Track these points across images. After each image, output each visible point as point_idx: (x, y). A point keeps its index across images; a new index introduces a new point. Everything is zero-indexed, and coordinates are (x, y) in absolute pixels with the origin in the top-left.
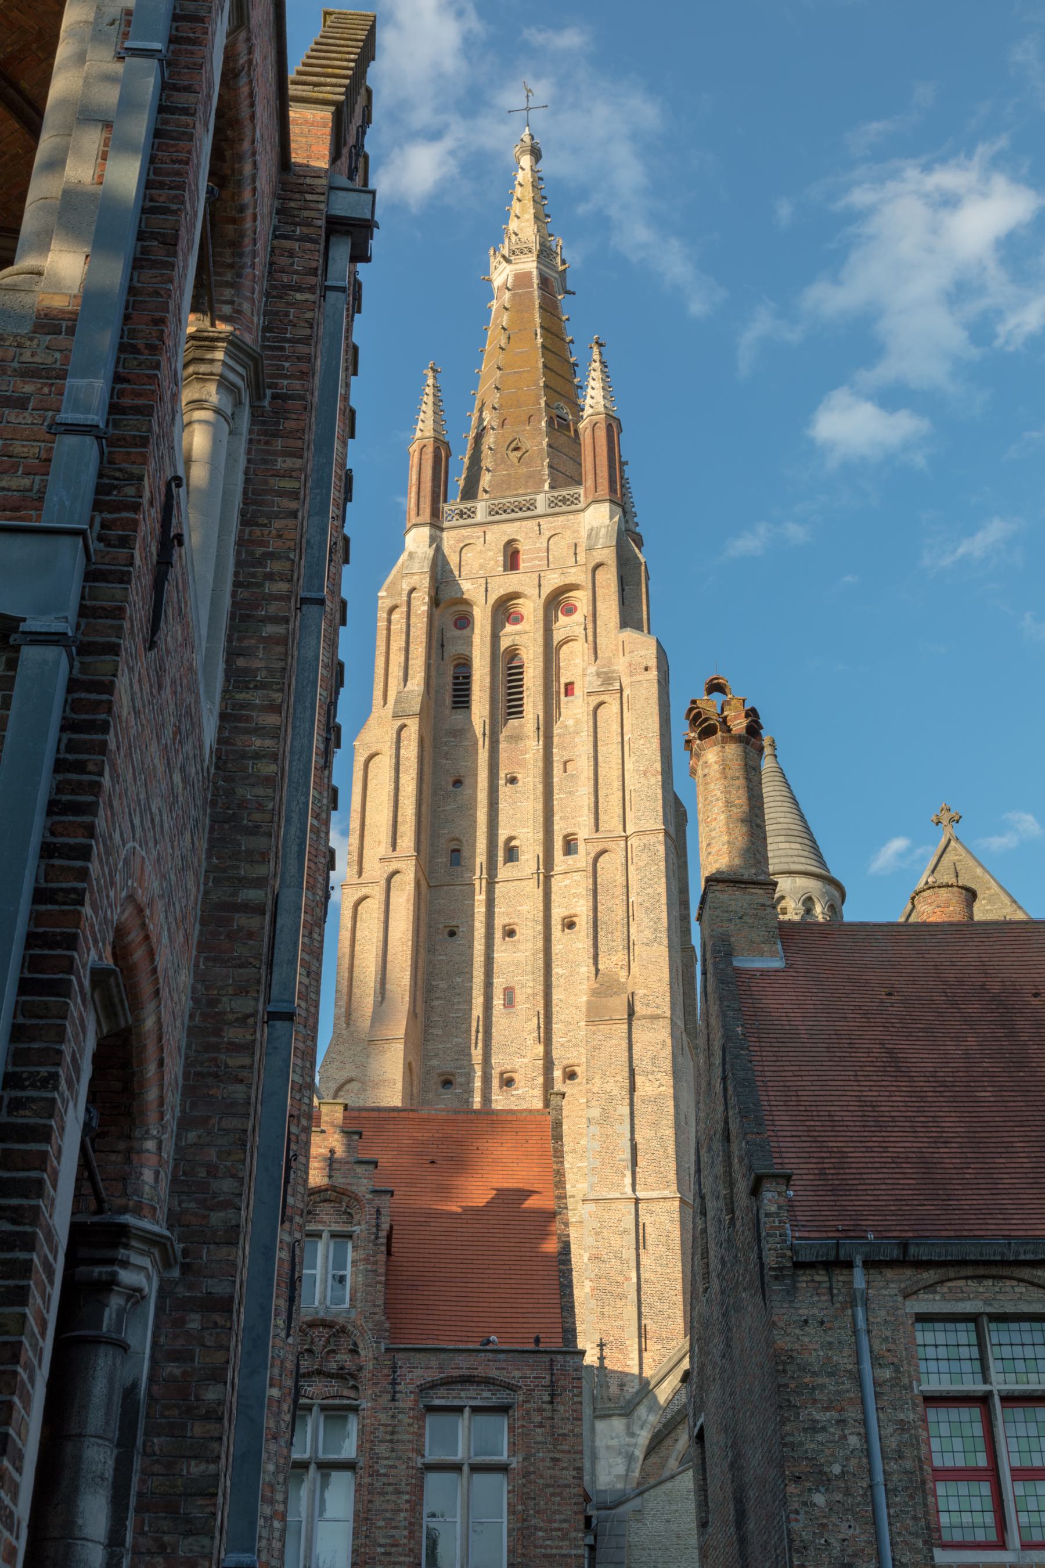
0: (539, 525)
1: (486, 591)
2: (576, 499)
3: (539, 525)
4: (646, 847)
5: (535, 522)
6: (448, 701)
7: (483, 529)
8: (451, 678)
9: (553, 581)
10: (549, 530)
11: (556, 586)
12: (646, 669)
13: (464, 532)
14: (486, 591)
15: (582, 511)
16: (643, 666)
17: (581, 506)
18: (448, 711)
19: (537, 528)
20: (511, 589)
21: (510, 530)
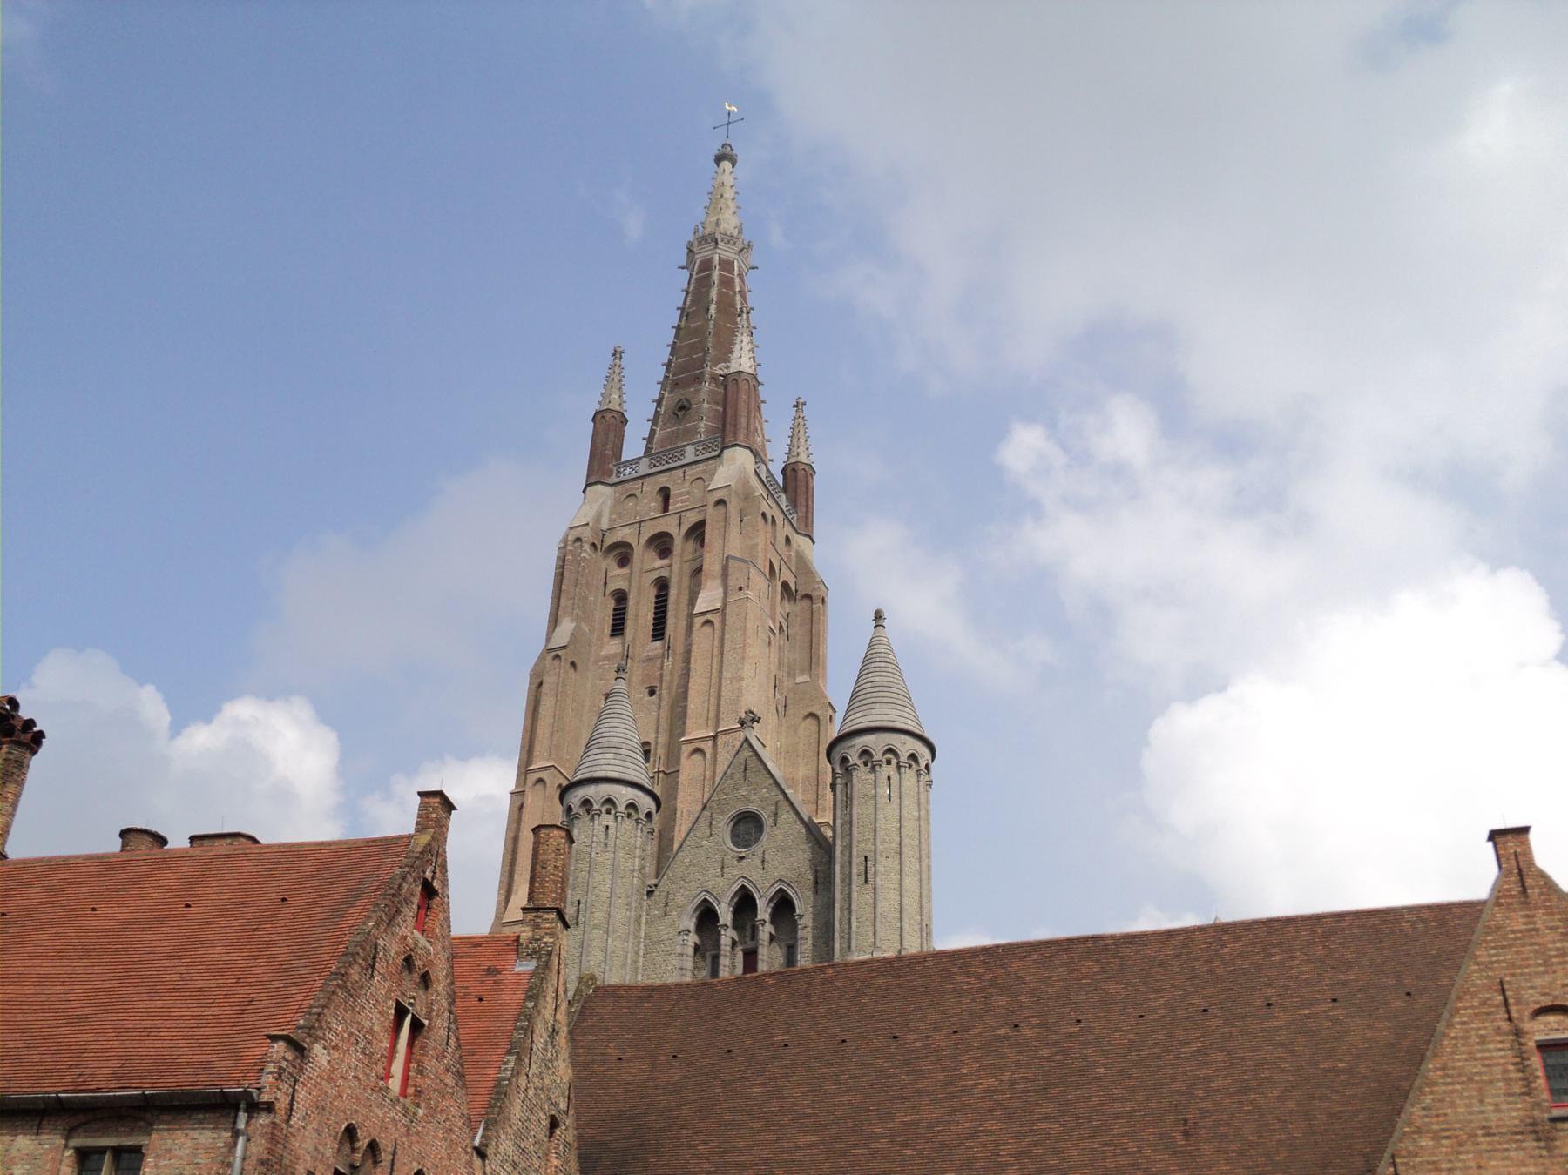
0: (684, 473)
1: (639, 533)
2: (716, 446)
3: (684, 473)
4: (726, 744)
5: (681, 470)
6: (608, 630)
7: (640, 482)
8: (612, 610)
9: (692, 518)
10: (691, 476)
11: (692, 524)
12: (740, 589)
13: (628, 486)
14: (639, 533)
15: (719, 455)
16: (738, 587)
17: (716, 453)
18: (606, 639)
19: (682, 475)
20: (659, 530)
21: (662, 480)
